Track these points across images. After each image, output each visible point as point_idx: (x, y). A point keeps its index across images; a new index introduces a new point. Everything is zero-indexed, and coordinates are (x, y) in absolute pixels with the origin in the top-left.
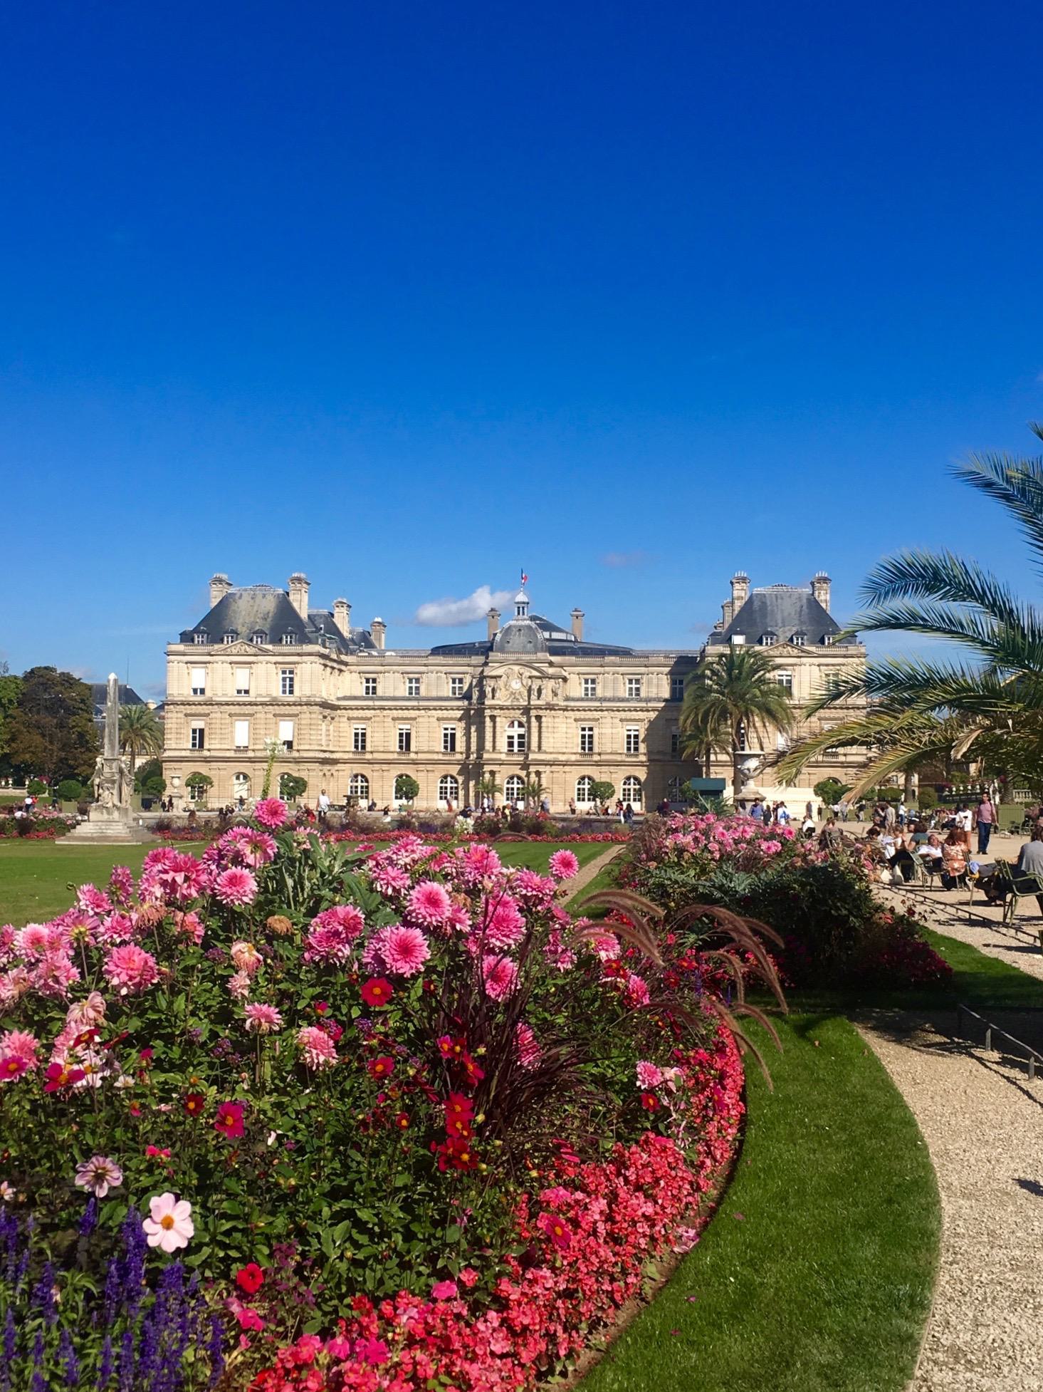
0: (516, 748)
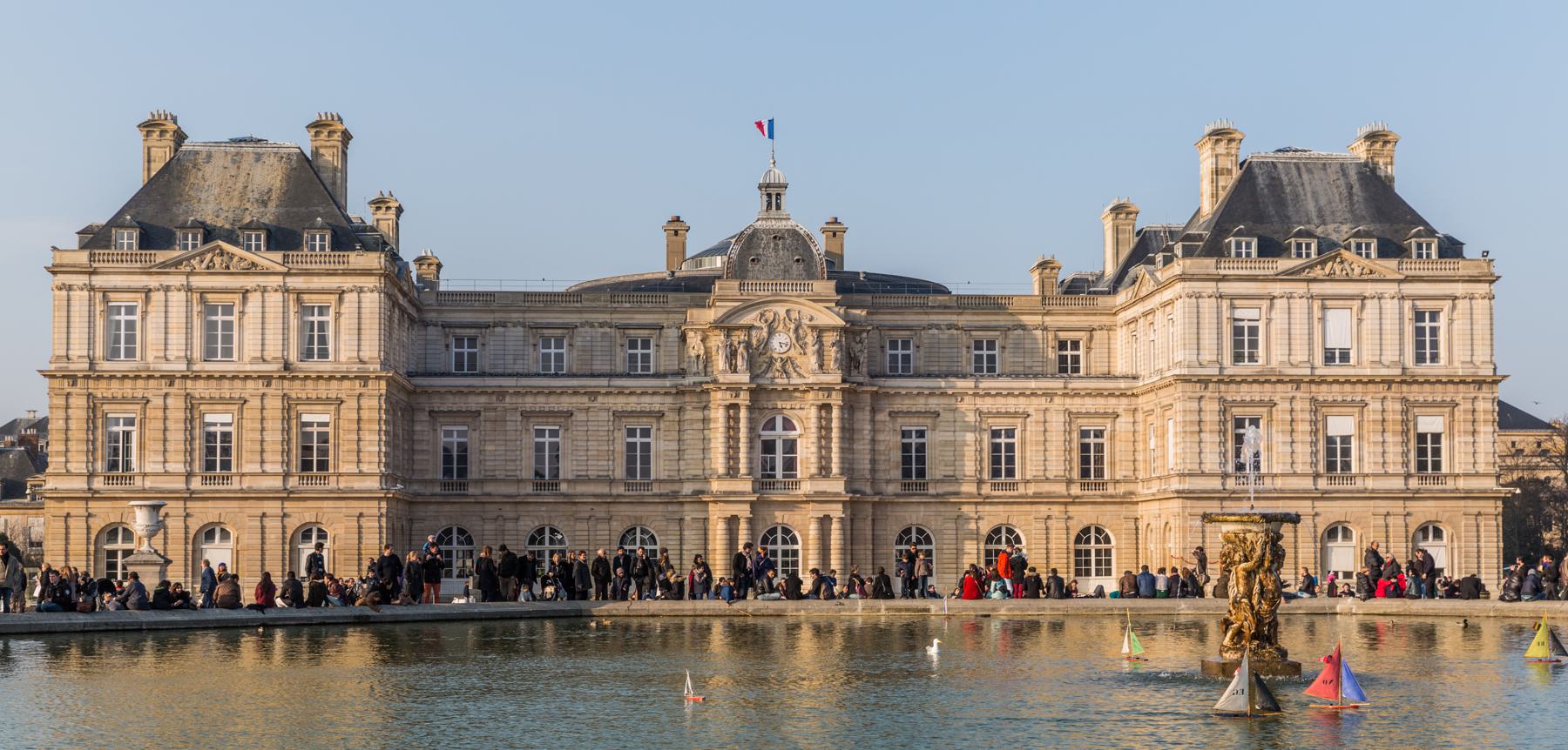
0: (779, 472)
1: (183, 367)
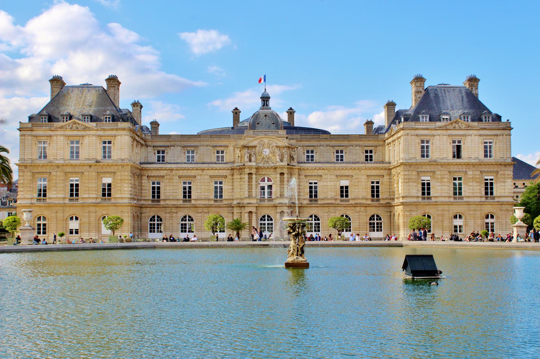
1: (63, 162)
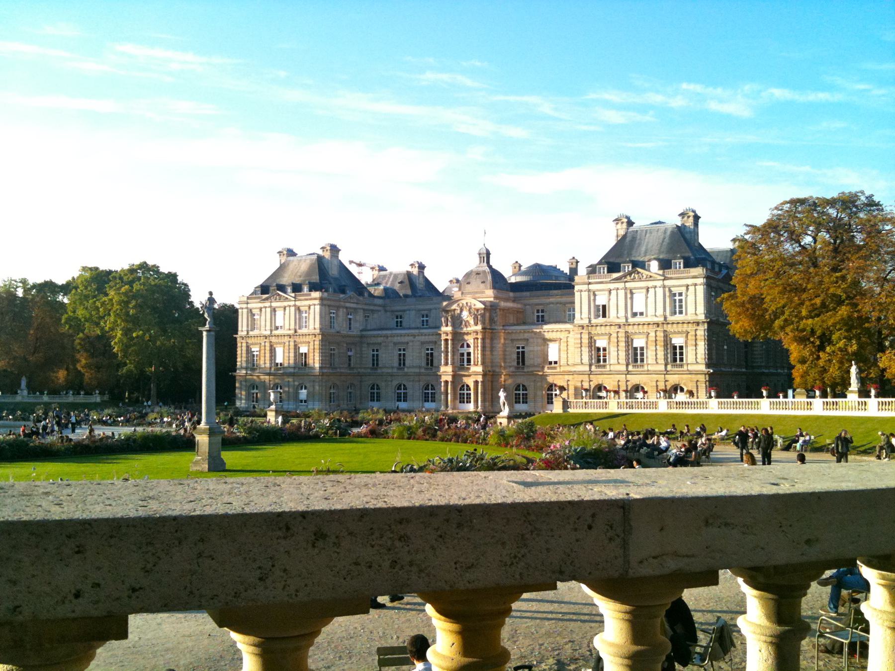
0: (465, 363)
